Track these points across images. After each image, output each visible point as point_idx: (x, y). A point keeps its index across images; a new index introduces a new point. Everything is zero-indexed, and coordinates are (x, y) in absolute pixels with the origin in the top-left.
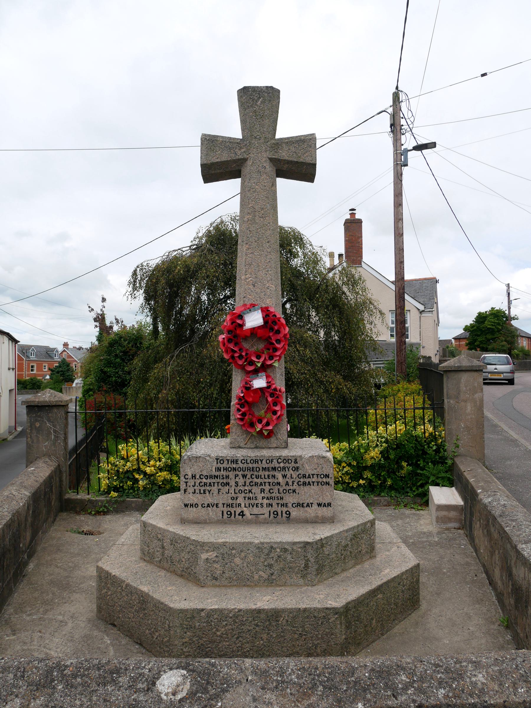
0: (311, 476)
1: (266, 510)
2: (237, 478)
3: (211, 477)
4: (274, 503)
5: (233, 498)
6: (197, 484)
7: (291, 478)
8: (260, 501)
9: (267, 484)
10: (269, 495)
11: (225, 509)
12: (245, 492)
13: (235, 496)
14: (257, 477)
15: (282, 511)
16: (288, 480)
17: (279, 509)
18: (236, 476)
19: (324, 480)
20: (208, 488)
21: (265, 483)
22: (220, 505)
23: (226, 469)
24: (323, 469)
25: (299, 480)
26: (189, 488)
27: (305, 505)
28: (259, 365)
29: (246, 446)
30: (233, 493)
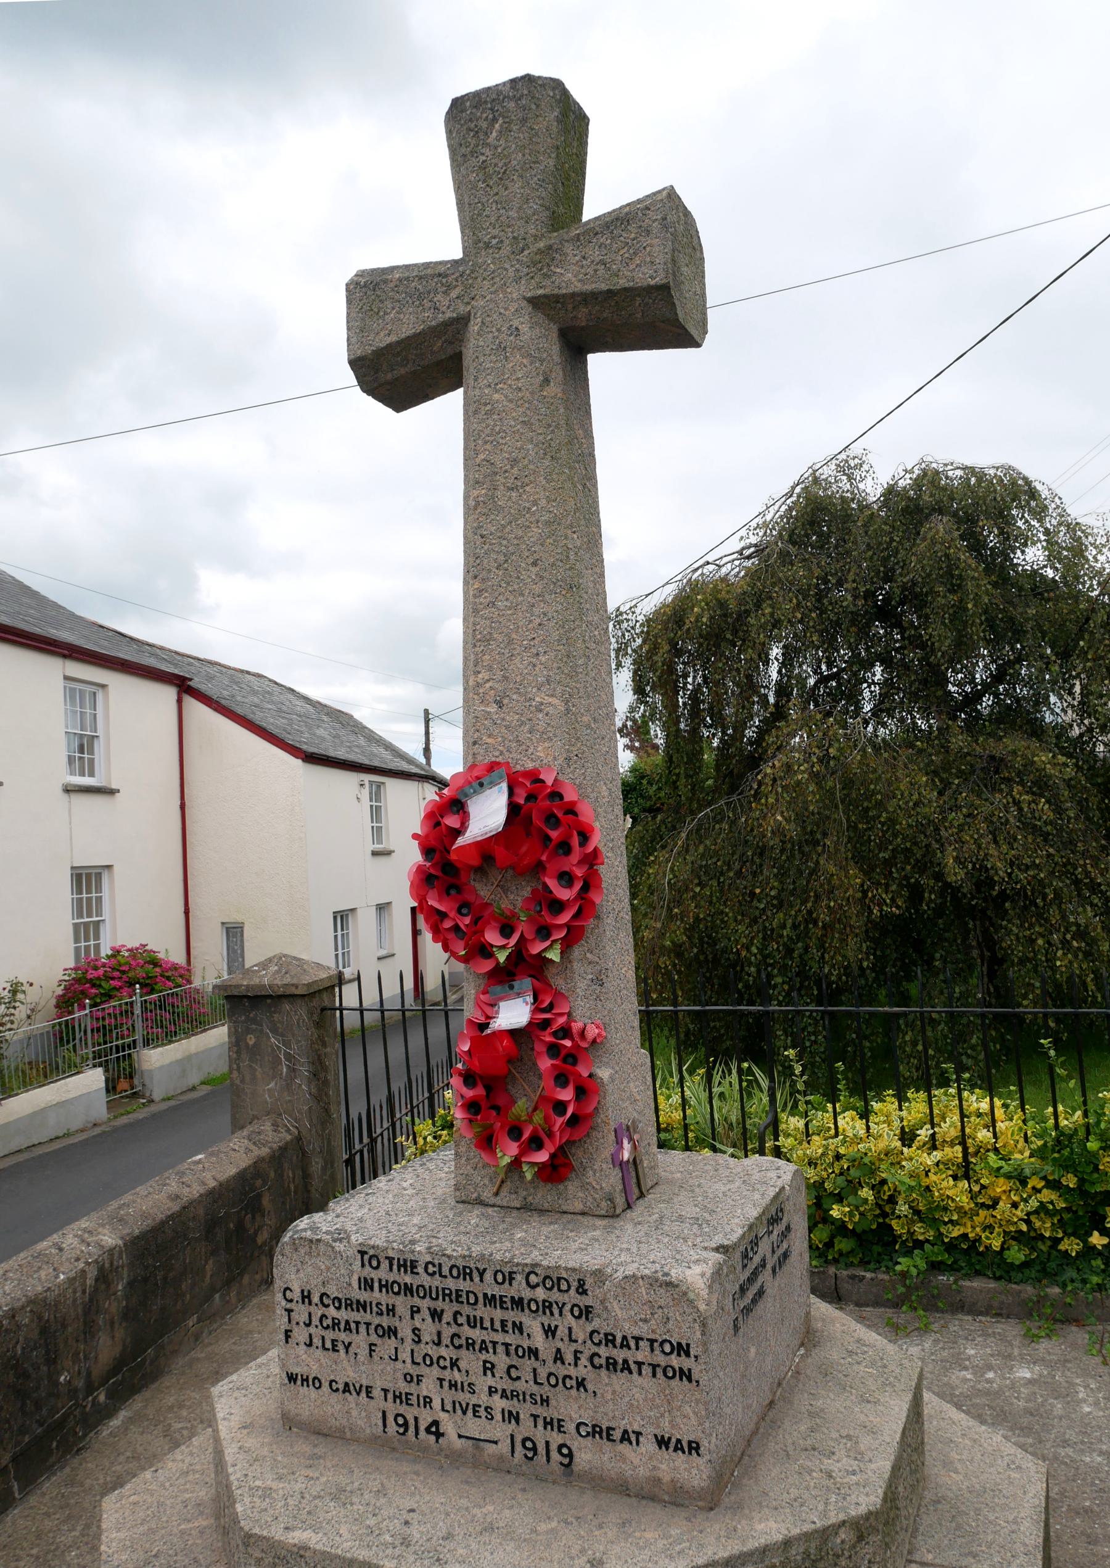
0: (632, 1344)
1: (500, 1430)
2: (416, 1316)
3: (349, 1304)
4: (525, 1410)
5: (408, 1378)
6: (315, 1321)
7: (571, 1340)
8: (483, 1399)
9: (500, 1349)
10: (508, 1385)
11: (392, 1408)
12: (442, 1363)
13: (414, 1371)
14: (472, 1322)
15: (547, 1443)
16: (560, 1345)
17: (540, 1435)
18: (415, 1311)
19: (675, 1361)
20: (343, 1336)
21: (495, 1343)
22: (377, 1393)
23: (386, 1286)
24: (670, 1325)
25: (595, 1349)
26: (296, 1330)
27: (617, 1435)
28: (502, 957)
29: (498, 1201)
30: (409, 1360)
